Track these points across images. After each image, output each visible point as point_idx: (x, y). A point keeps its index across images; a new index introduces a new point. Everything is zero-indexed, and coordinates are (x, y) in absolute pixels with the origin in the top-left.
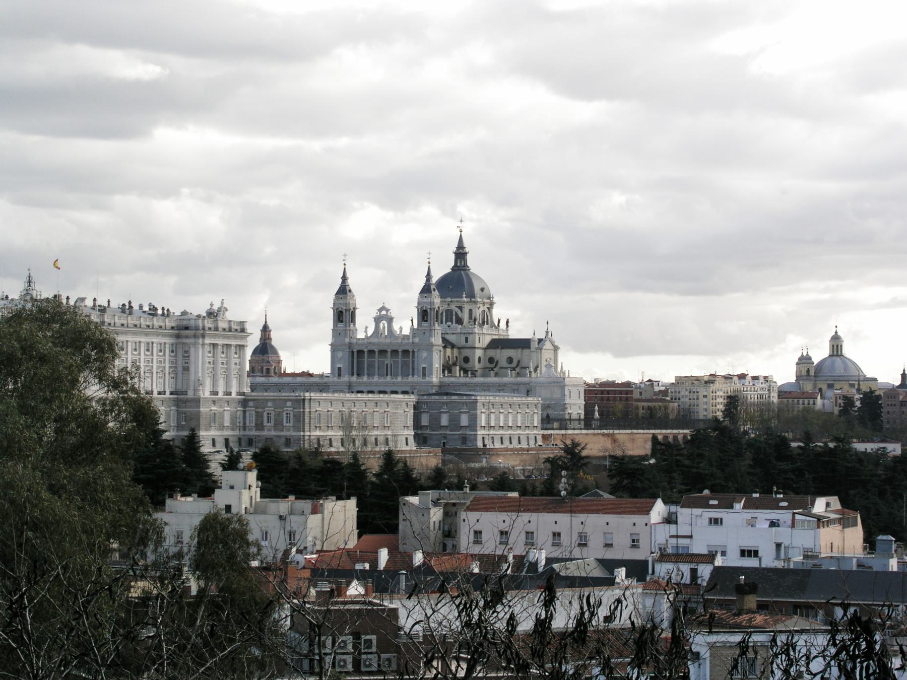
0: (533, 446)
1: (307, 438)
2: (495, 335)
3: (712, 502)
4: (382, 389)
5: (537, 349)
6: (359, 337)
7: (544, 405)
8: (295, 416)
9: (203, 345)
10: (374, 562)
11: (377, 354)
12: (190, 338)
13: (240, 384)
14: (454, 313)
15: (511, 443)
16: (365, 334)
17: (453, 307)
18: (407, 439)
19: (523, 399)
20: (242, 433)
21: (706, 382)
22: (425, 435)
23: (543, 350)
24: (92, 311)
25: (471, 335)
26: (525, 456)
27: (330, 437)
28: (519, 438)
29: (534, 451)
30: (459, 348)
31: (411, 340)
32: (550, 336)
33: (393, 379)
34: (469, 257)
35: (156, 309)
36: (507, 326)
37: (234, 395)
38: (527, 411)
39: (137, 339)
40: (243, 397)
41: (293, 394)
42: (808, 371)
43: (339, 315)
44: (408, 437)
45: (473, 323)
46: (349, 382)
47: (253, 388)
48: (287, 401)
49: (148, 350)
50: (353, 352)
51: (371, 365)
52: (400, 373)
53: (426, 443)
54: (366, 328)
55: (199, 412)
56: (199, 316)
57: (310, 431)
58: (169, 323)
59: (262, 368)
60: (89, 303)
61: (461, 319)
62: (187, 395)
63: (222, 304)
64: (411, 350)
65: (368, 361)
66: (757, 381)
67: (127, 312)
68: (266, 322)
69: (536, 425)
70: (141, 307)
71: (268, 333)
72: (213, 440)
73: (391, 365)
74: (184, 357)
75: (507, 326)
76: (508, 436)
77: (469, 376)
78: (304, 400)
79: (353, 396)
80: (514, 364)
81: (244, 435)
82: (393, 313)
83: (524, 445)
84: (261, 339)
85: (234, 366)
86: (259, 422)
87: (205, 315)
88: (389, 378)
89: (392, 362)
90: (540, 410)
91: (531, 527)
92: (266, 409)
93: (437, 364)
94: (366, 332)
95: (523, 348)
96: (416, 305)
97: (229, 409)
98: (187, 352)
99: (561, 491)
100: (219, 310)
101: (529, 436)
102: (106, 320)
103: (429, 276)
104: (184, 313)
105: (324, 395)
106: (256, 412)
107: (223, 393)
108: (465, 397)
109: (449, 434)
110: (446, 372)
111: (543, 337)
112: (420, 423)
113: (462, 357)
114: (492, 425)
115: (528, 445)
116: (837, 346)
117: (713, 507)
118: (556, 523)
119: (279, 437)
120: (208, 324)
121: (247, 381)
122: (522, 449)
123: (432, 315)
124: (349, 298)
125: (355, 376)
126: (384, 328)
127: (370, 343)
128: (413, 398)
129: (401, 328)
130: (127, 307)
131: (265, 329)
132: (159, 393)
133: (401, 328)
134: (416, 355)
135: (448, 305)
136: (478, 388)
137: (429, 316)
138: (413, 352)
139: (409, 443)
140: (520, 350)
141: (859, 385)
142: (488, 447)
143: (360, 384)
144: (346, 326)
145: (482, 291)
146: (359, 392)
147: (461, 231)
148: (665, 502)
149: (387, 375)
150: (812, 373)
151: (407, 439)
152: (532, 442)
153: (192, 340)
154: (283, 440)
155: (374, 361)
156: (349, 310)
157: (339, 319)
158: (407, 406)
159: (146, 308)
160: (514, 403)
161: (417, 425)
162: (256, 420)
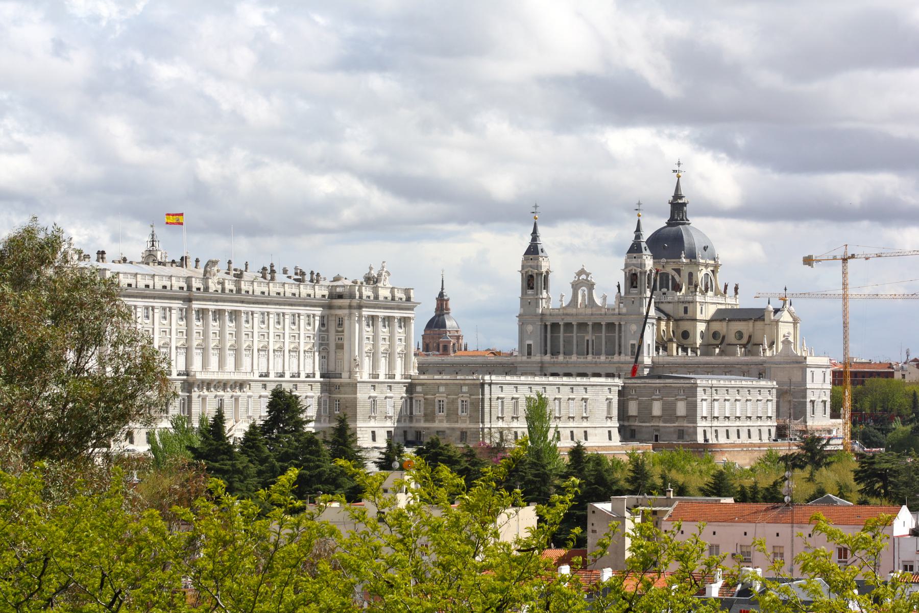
0: (767, 441)
1: (486, 430)
2: (721, 304)
4: (581, 371)
7: (781, 389)
8: (472, 404)
11: (575, 327)
12: (345, 309)
13: (406, 366)
14: (670, 277)
15: (739, 437)
17: (669, 270)
18: (610, 432)
19: (754, 383)
20: (408, 424)
22: (633, 428)
23: (780, 323)
24: (227, 277)
25: (691, 304)
26: (756, 453)
27: (515, 430)
28: (749, 431)
30: (675, 320)
31: (617, 311)
32: (788, 306)
33: (595, 358)
34: (687, 209)
35: (303, 274)
36: (736, 293)
40: (410, 381)
41: (470, 377)
43: (529, 280)
45: (694, 290)
46: (542, 363)
47: (422, 369)
48: (439, 385)
50: (546, 326)
51: (568, 342)
52: (603, 351)
53: (634, 437)
54: (562, 296)
55: (356, 398)
56: (355, 282)
57: (490, 422)
58: (321, 291)
59: (438, 345)
60: (222, 266)
61: (679, 285)
63: (383, 267)
64: (617, 323)
65: (564, 337)
67: (269, 277)
68: (442, 289)
69: (769, 415)
70: (285, 271)
72: (373, 433)
73: (593, 341)
74: (337, 331)
75: (736, 293)
76: (736, 429)
77: (689, 354)
78: (482, 385)
79: (543, 380)
80: (744, 341)
81: (411, 427)
82: (593, 279)
83: (755, 439)
84: (437, 310)
85: (398, 343)
86: (429, 412)
87: (363, 280)
88: (590, 358)
89: (594, 338)
90: (775, 396)
91: (715, 540)
93: (649, 338)
94: (561, 301)
95: (755, 320)
96: (623, 268)
98: (340, 324)
100: (380, 275)
101: (762, 428)
103: (638, 229)
104: (337, 279)
108: (682, 381)
109: (662, 427)
110: (661, 351)
111: (780, 307)
112: (627, 412)
113: (680, 331)
114: (715, 416)
115: (760, 439)
119: (453, 429)
120: (367, 292)
121: (414, 360)
124: (541, 259)
125: (548, 356)
126: (583, 296)
127: (567, 314)
128: (619, 382)
129: (605, 298)
130: (269, 271)
133: (605, 298)
134: (623, 328)
135: (663, 267)
136: (699, 369)
137: (638, 283)
138: (620, 325)
139: (613, 438)
140: (751, 323)
142: (710, 442)
143: (554, 363)
144: (537, 294)
145: (705, 250)
146: (553, 375)
147: (679, 177)
149: (588, 354)
151: (610, 432)
152: (765, 437)
153: (346, 311)
154: (458, 433)
155: (573, 337)
156: (542, 274)
157: (529, 285)
158: (610, 392)
159: (291, 272)
161: (623, 415)
162: (425, 409)
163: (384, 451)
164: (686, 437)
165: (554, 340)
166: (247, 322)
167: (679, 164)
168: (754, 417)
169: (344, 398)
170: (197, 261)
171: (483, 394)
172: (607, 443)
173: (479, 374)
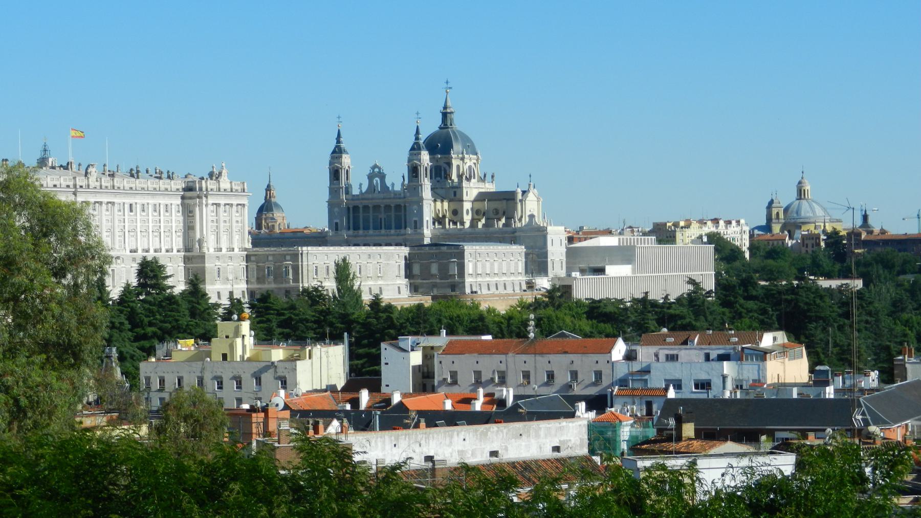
3: (669, 340)
4: (377, 242)
5: (521, 201)
6: (353, 194)
9: (207, 205)
10: (355, 402)
14: (443, 169)
15: (497, 289)
16: (359, 190)
18: (399, 288)
19: (508, 247)
21: (682, 228)
23: (526, 202)
25: (459, 190)
28: (505, 284)
29: (518, 296)
31: (402, 195)
34: (454, 116)
35: (161, 173)
37: (236, 250)
38: (512, 259)
39: (145, 201)
40: (246, 253)
42: (778, 214)
44: (401, 286)
49: (155, 211)
51: (366, 220)
54: (361, 185)
62: (192, 252)
64: (403, 205)
66: (728, 226)
68: (270, 182)
69: (520, 272)
70: (147, 172)
71: (272, 192)
72: (219, 293)
74: (188, 216)
76: (494, 283)
77: (459, 227)
78: (302, 254)
83: (509, 290)
84: (266, 198)
90: (524, 257)
92: (267, 263)
95: (508, 200)
97: (232, 264)
98: (191, 212)
99: (529, 333)
102: (115, 184)
103: (417, 132)
105: (320, 248)
106: (257, 266)
107: (226, 250)
108: (453, 247)
110: (436, 224)
111: (526, 189)
114: (479, 273)
115: (514, 290)
116: (804, 190)
117: (670, 344)
118: (525, 362)
119: (280, 289)
120: (211, 184)
122: (508, 295)
123: (422, 171)
127: (363, 199)
128: (405, 251)
131: (268, 189)
132: (156, 251)
133: (393, 185)
134: (407, 209)
135: (437, 161)
138: (405, 206)
141: (825, 226)
146: (355, 245)
148: (625, 340)
149: (381, 228)
150: (782, 216)
151: (399, 288)
157: (335, 176)
159: (152, 172)
160: (499, 252)
161: (409, 274)
162: (257, 273)
163: (227, 306)
164: (457, 289)
165: (356, 219)
166: (120, 211)
167: (447, 82)
168: (508, 274)
169: (196, 267)
170: (80, 165)
171: (302, 262)
172: (398, 296)
173: (298, 246)
